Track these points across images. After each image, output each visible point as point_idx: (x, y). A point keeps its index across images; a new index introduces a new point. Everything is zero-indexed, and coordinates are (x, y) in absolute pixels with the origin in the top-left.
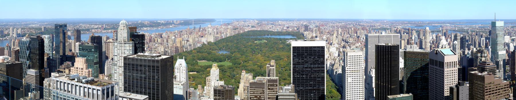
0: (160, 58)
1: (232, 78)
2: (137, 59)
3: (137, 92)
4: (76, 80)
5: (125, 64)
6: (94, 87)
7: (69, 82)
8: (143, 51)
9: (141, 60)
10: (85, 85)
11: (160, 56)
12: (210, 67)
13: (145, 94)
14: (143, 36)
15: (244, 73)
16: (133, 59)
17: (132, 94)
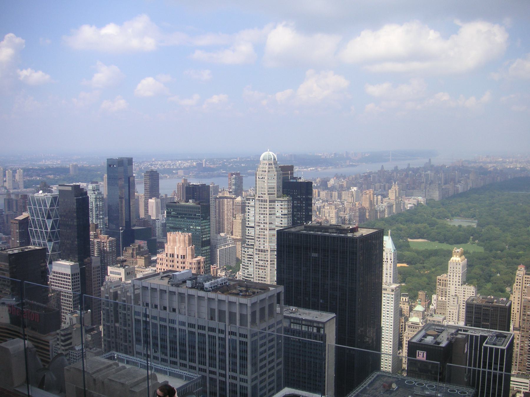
0: (357, 234)
1: (488, 281)
2: (307, 235)
3: (307, 306)
4: (189, 283)
6: (233, 299)
7: (173, 289)
8: (310, 219)
9: (316, 236)
10: (212, 295)
12: (450, 254)
13: (331, 311)
14: (307, 187)
15: (521, 271)
16: (297, 235)
17: (301, 310)
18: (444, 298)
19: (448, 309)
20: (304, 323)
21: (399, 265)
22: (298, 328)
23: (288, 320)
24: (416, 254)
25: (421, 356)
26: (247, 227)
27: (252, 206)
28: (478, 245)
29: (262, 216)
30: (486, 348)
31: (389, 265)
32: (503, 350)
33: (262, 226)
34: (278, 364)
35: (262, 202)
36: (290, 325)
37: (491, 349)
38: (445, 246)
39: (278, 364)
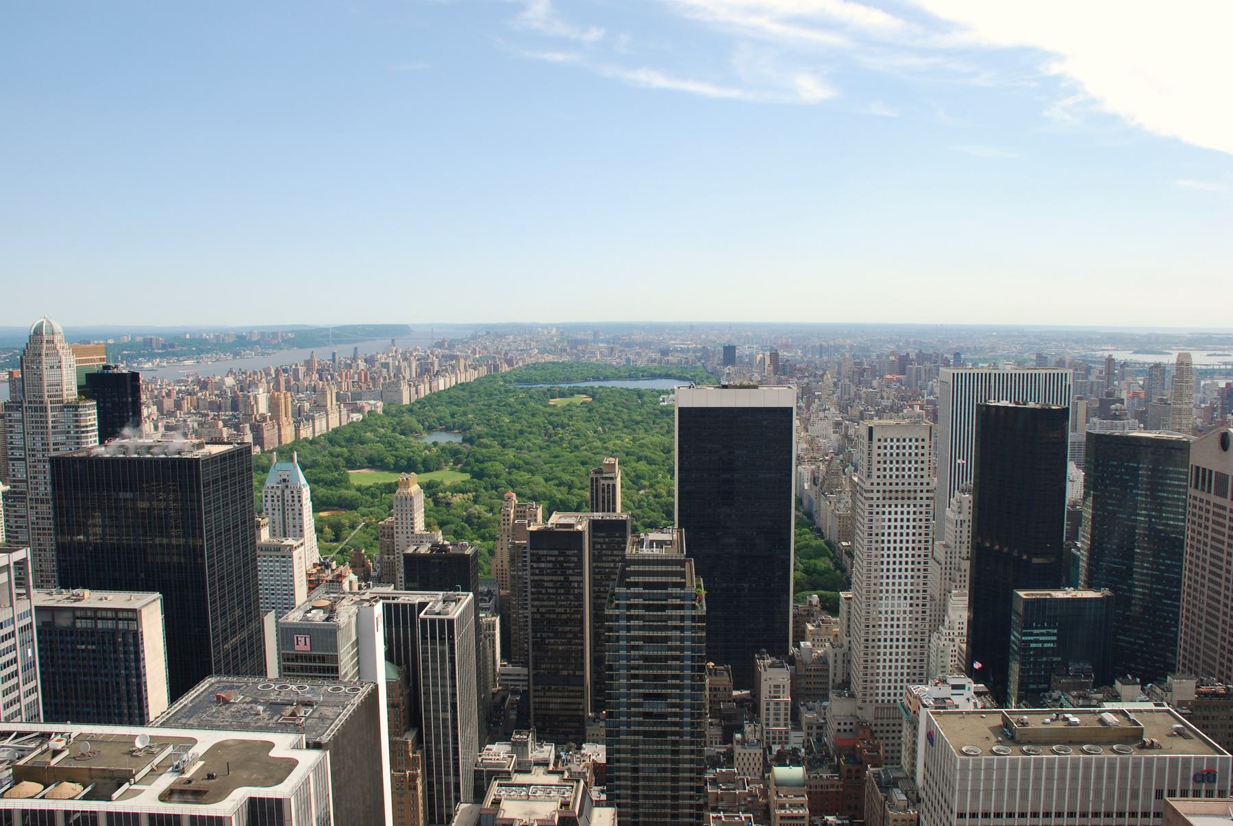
5: (56, 484)
11: (200, 446)
18: (391, 557)
19: (398, 575)
20: (99, 614)
21: (322, 514)
22: (89, 625)
23: (69, 615)
24: (359, 494)
25: (302, 645)
26: (11, 459)
27: (16, 421)
28: (462, 471)
29: (38, 438)
30: (424, 621)
31: (297, 512)
32: (451, 622)
33: (39, 456)
34: (30, 692)
35: (36, 410)
36: (74, 623)
37: (433, 621)
38: (402, 476)
39: (30, 692)
